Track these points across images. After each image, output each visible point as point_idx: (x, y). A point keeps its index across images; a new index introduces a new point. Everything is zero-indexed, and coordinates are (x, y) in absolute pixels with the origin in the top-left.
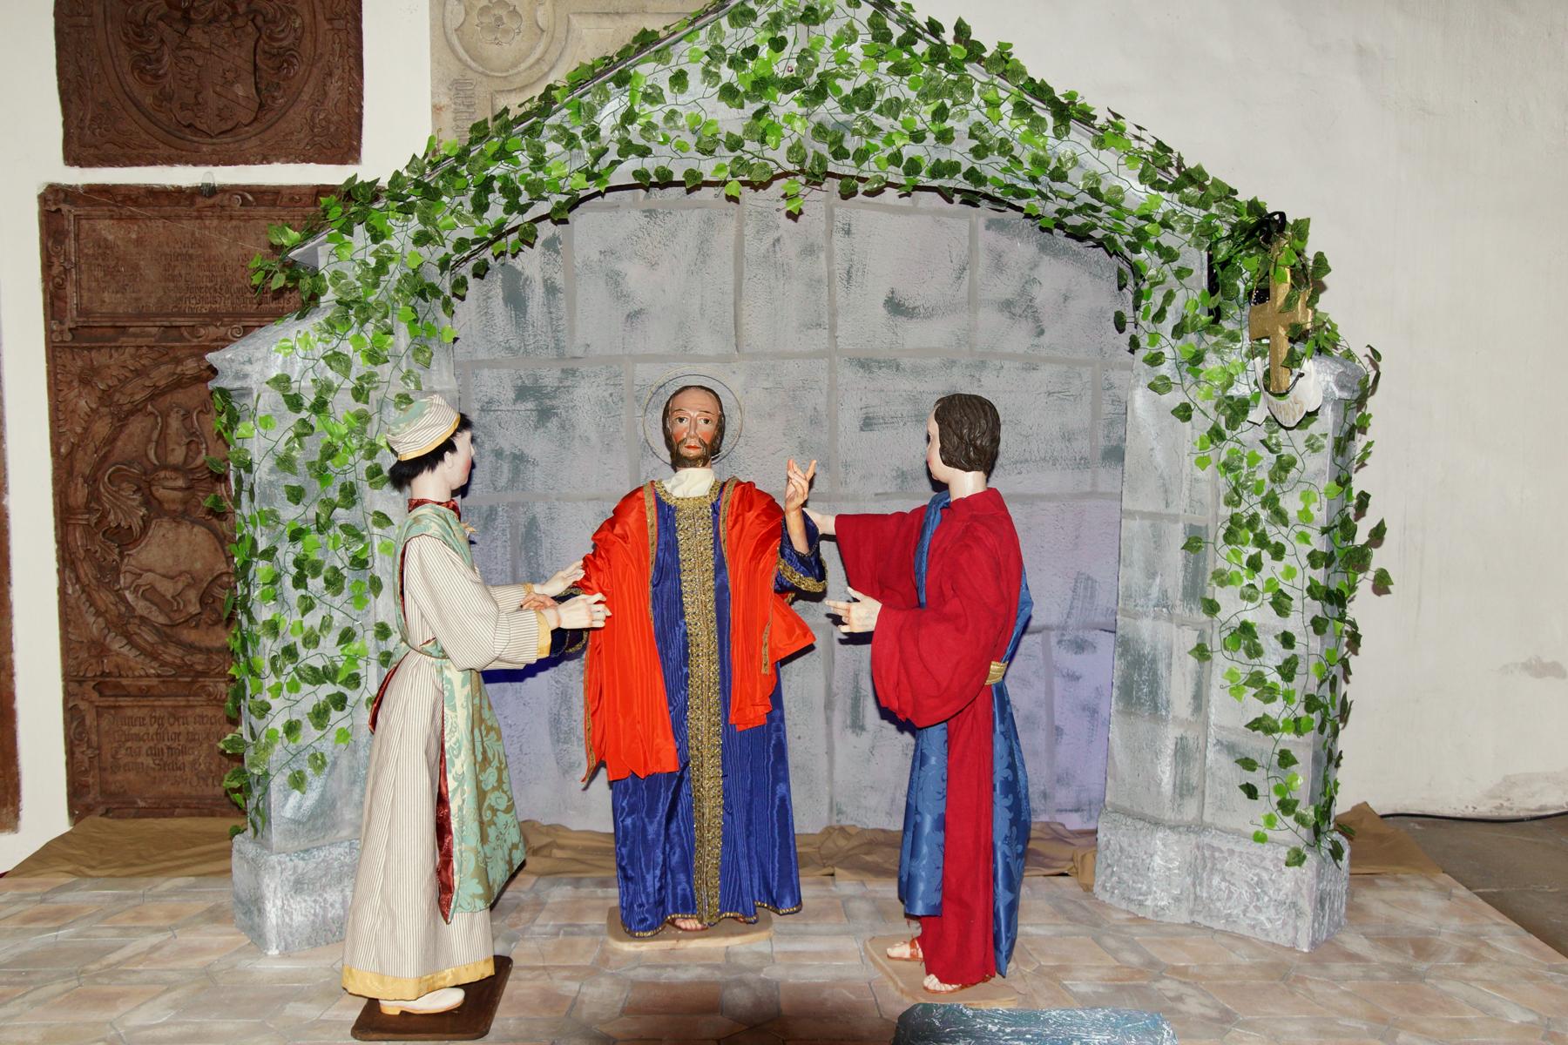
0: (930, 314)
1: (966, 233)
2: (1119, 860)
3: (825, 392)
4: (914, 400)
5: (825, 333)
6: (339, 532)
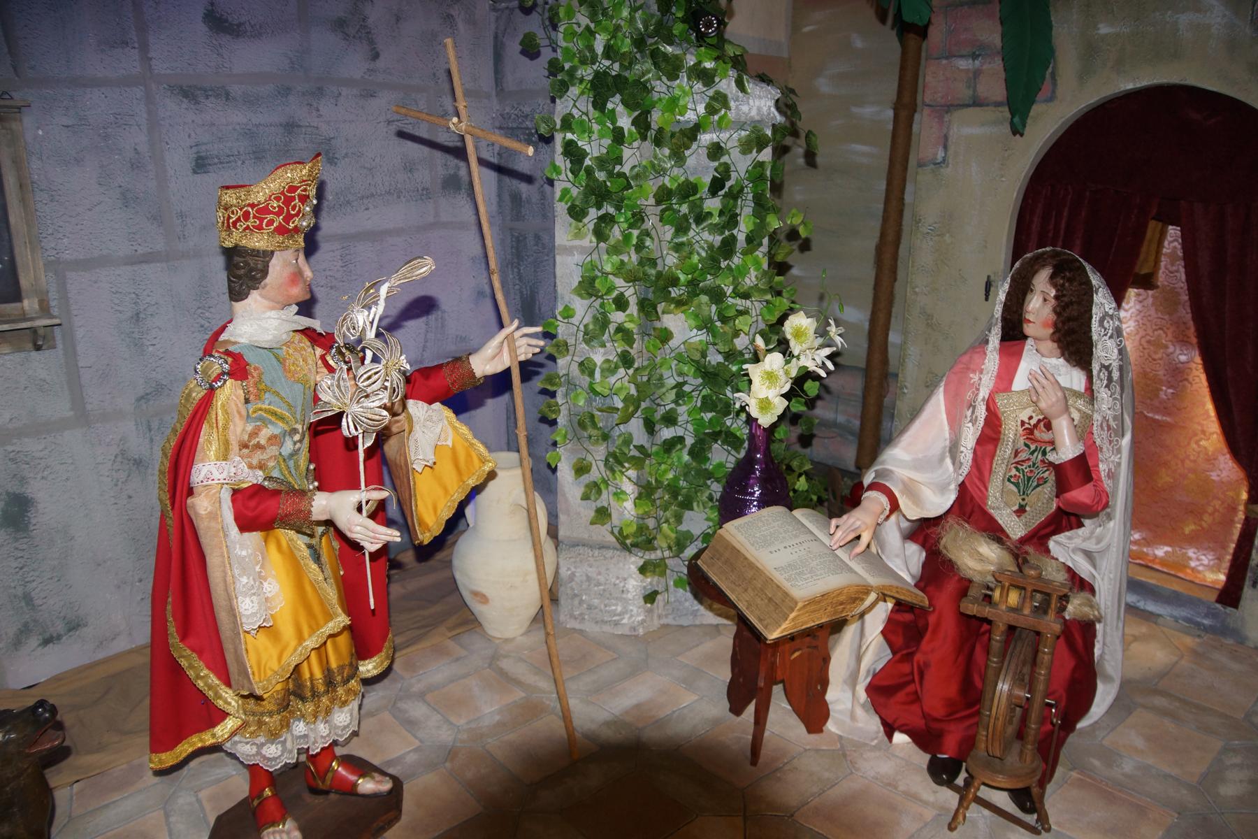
4: (249, 133)
5: (135, 54)
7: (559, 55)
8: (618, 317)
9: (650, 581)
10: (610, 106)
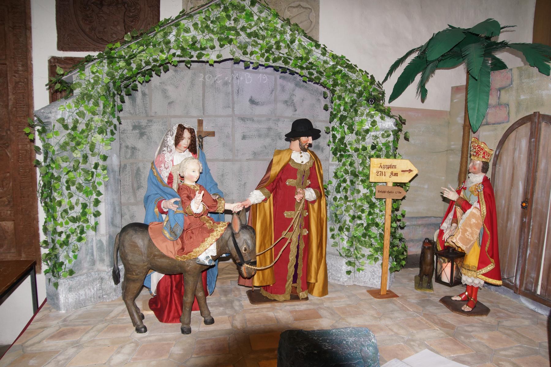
0: (263, 104)
1: (274, 80)
2: (331, 268)
3: (231, 127)
4: (258, 130)
6: (81, 171)
7: (333, 110)
8: (344, 185)
9: (349, 268)
10: (343, 124)
